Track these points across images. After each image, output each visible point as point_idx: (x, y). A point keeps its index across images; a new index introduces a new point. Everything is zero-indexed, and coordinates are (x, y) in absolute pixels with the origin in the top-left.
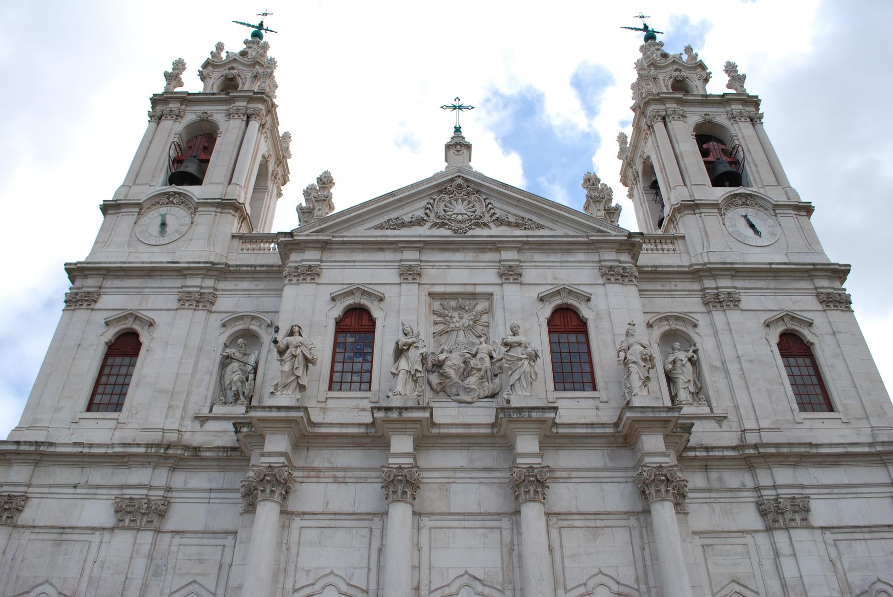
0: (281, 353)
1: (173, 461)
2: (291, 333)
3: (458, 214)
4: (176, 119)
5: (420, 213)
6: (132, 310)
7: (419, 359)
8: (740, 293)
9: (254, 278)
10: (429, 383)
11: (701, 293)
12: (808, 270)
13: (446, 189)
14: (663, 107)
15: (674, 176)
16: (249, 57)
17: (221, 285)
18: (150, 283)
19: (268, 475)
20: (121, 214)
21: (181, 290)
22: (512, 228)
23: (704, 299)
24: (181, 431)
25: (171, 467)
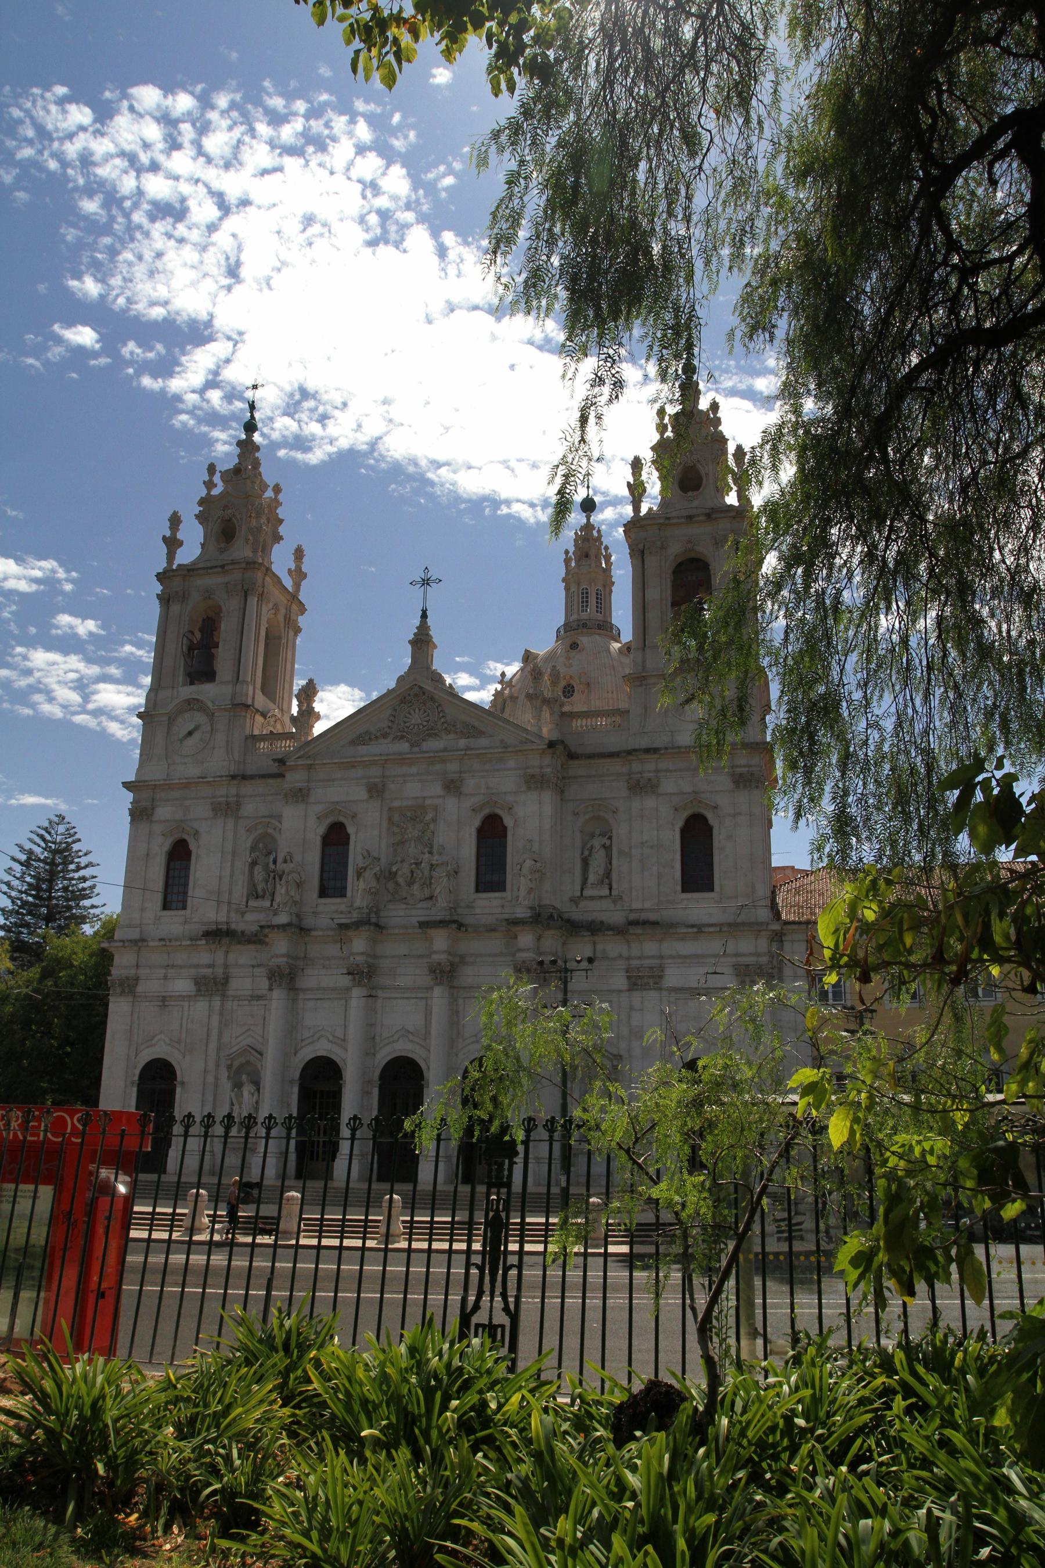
2: (285, 861)
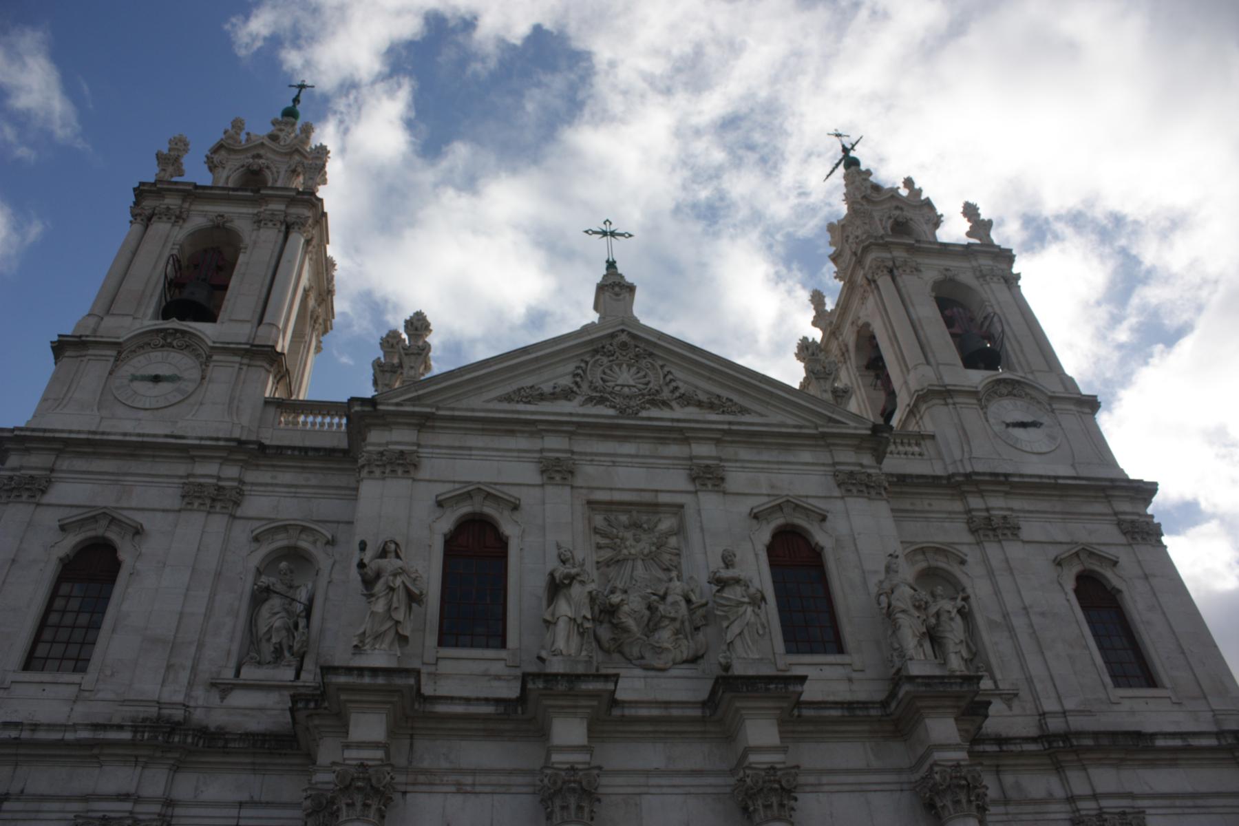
0: (369, 582)
1: (177, 755)
2: (383, 554)
3: (623, 386)
4: (175, 222)
5: (566, 381)
6: (105, 507)
7: (587, 601)
8: (1018, 517)
9: (303, 468)
10: (598, 640)
11: (965, 516)
12: (1103, 489)
13: (603, 347)
14: (889, 256)
15: (912, 353)
16: (282, 143)
17: (251, 476)
19: (358, 779)
20: (88, 358)
21: (186, 481)
22: (703, 411)
23: (972, 525)
24: (188, 707)
25: (173, 765)
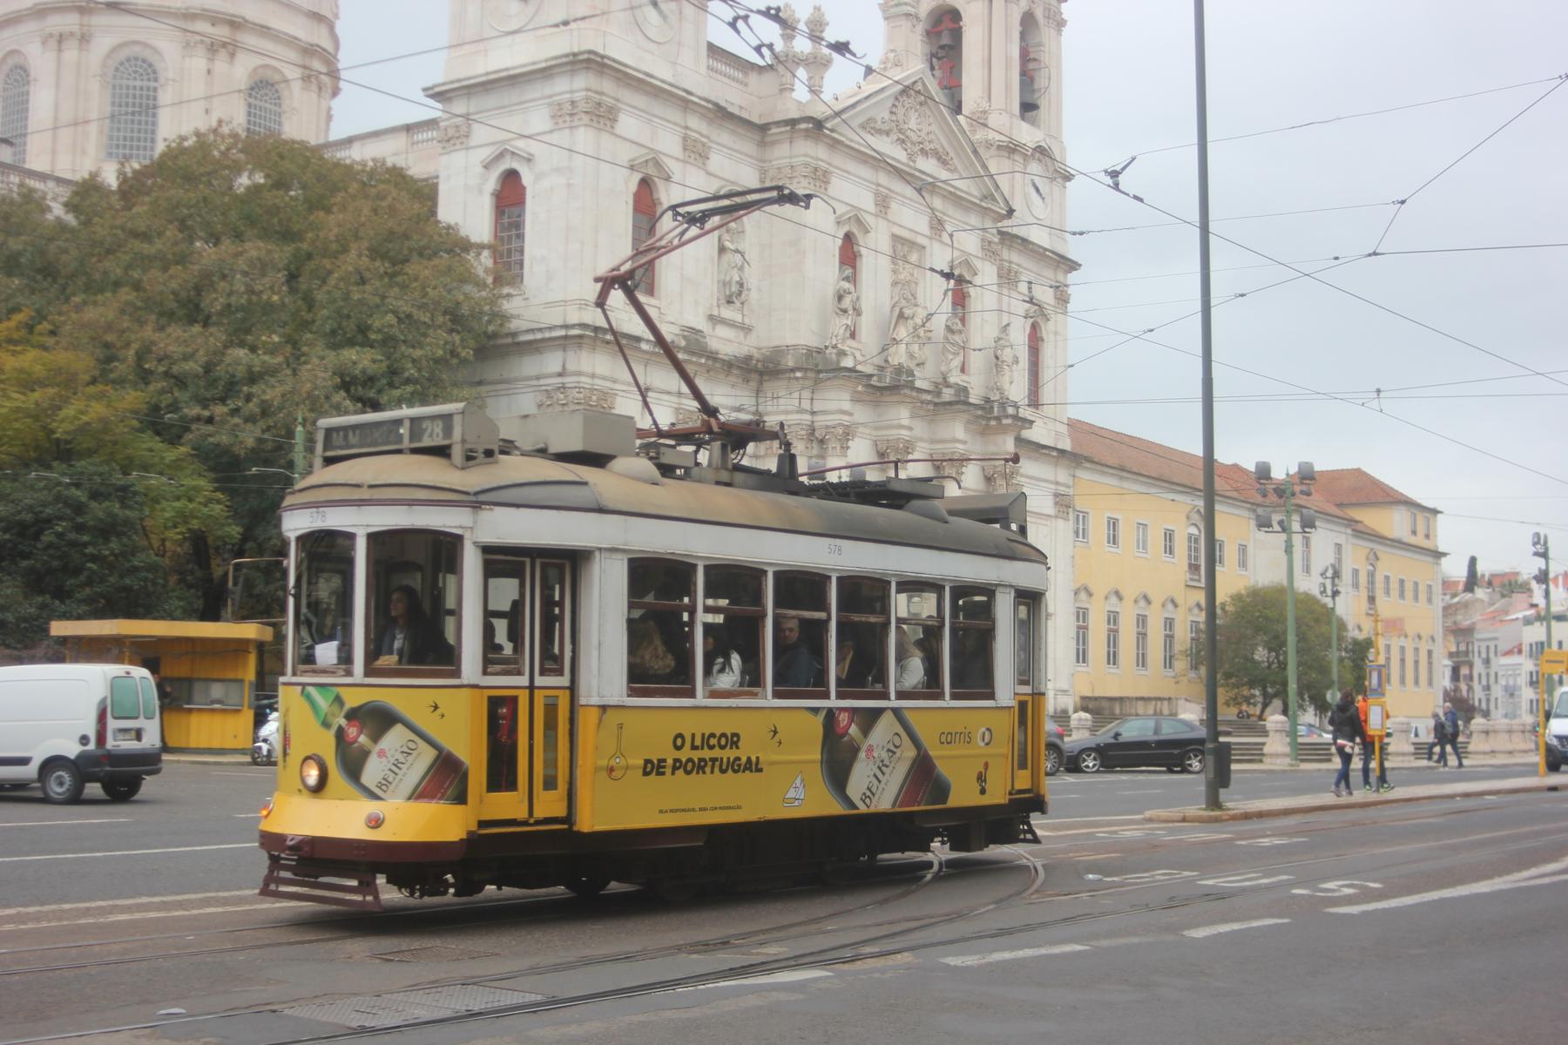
18: (658, 108)
